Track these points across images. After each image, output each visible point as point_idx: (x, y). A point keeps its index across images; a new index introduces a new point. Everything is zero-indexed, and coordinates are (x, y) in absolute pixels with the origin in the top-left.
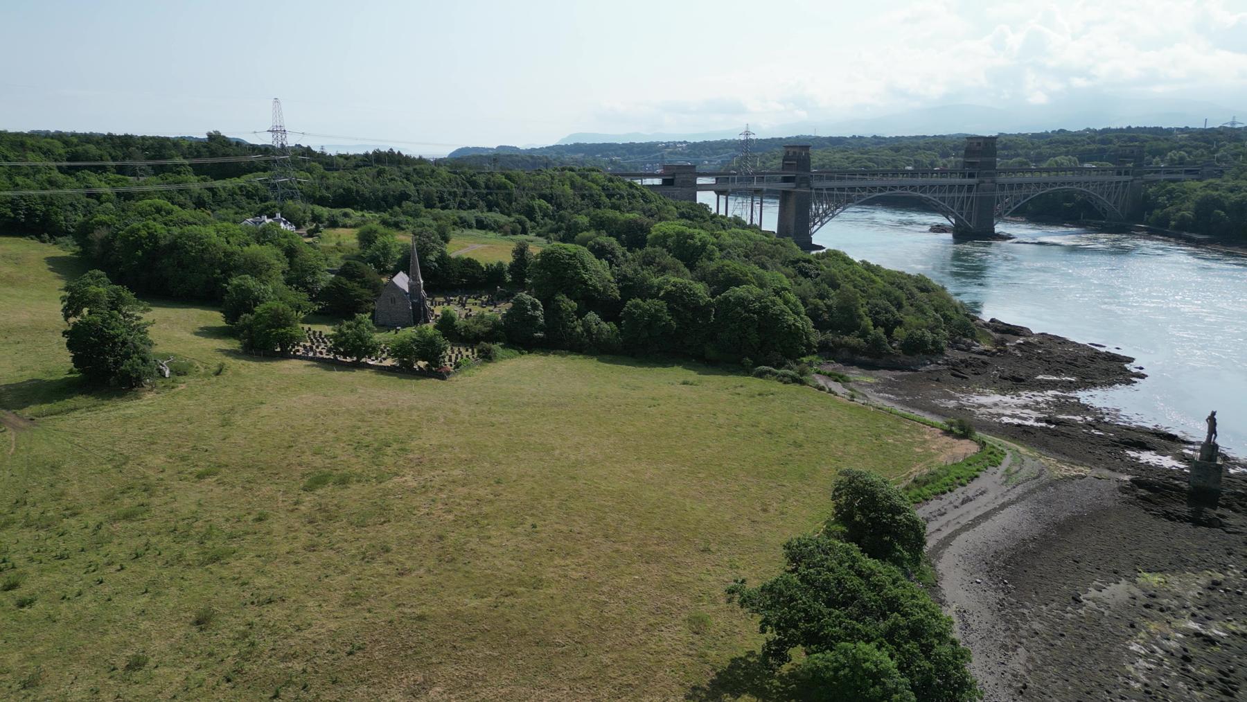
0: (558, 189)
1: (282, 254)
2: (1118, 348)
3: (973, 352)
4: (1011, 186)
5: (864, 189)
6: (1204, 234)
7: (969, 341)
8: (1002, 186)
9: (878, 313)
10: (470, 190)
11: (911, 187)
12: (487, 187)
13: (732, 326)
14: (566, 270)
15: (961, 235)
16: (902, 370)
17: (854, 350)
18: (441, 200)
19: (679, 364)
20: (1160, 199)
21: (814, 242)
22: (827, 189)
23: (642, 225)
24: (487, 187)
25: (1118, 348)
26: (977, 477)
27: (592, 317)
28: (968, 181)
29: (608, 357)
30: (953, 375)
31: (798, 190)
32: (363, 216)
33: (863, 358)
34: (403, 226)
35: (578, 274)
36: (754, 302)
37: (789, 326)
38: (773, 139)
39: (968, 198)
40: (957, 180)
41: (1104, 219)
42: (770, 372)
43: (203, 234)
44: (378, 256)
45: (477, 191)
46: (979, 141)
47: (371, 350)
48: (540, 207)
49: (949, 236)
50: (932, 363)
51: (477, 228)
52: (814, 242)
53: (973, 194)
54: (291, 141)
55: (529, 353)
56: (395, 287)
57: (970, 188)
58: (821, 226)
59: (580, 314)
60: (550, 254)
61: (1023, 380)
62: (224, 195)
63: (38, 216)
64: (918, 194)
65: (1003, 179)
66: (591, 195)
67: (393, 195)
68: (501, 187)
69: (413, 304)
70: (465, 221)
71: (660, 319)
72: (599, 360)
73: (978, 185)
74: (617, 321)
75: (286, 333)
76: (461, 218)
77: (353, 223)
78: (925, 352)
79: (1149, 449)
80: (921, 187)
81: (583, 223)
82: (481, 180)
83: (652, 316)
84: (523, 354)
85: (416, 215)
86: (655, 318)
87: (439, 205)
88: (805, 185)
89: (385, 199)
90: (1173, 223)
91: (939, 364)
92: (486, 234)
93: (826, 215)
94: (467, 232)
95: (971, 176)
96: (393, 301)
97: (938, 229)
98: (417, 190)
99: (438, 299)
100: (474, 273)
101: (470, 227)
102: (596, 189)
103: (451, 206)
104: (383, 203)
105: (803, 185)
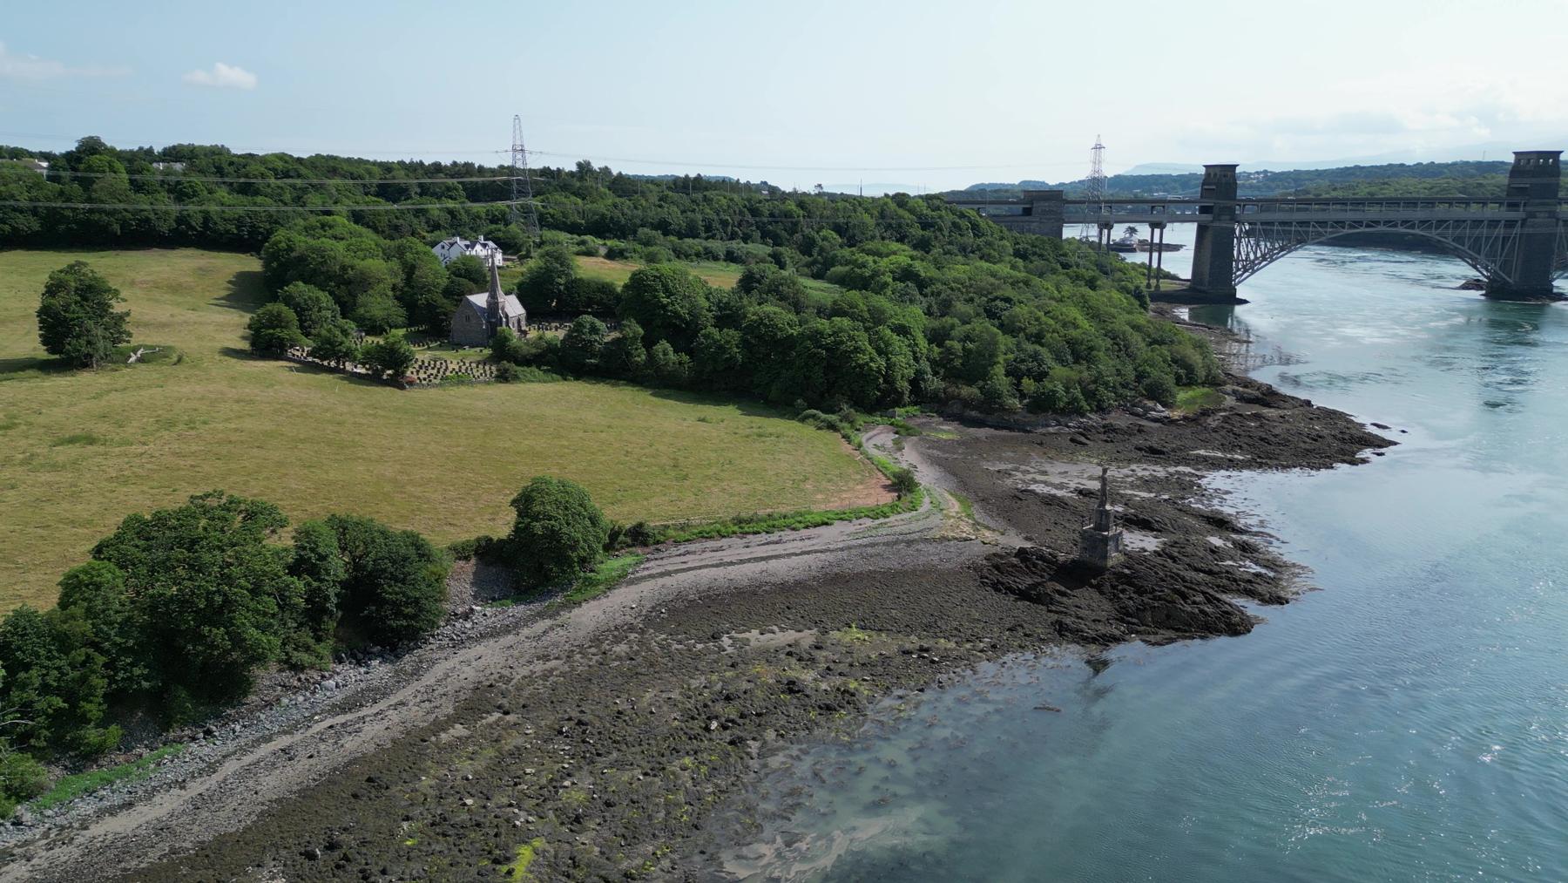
2: (1403, 432)
3: (1147, 419)
5: (1323, 224)
7: (1150, 404)
9: (1023, 361)
10: (749, 217)
12: (772, 215)
15: (1496, 291)
16: (1011, 429)
17: (967, 403)
18: (708, 228)
19: (734, 404)
21: (1238, 296)
22: (1283, 223)
24: (772, 215)
25: (1403, 432)
26: (827, 524)
27: (663, 346)
28: (1512, 215)
29: (666, 392)
30: (1072, 440)
31: (1217, 224)
33: (973, 413)
34: (628, 255)
35: (655, 297)
36: (830, 336)
37: (861, 366)
38: (1390, 165)
39: (1505, 239)
40: (1492, 211)
42: (814, 416)
43: (328, 247)
45: (757, 219)
46: (1529, 157)
47: (348, 355)
49: (1476, 294)
50: (1059, 424)
51: (725, 260)
52: (1238, 296)
53: (1517, 230)
54: (535, 163)
55: (577, 379)
56: (470, 304)
57: (1510, 224)
58: (1252, 274)
59: (649, 342)
61: (1163, 453)
62: (465, 218)
63: (261, 233)
64: (1401, 230)
66: (900, 226)
68: (788, 215)
69: (489, 322)
70: (711, 252)
72: (653, 395)
73: (1524, 221)
74: (690, 353)
75: (272, 334)
76: (706, 249)
78: (1055, 411)
79: (1152, 530)
80: (1423, 222)
82: (765, 209)
83: (721, 347)
84: (566, 380)
85: (647, 243)
86: (721, 349)
87: (703, 235)
88: (1228, 217)
91: (1068, 427)
92: (727, 266)
93: (1264, 259)
94: (712, 264)
95: (1513, 206)
96: (468, 318)
97: (1557, 287)
99: (553, 325)
100: (602, 299)
101: (716, 258)
103: (718, 236)
105: (1223, 217)
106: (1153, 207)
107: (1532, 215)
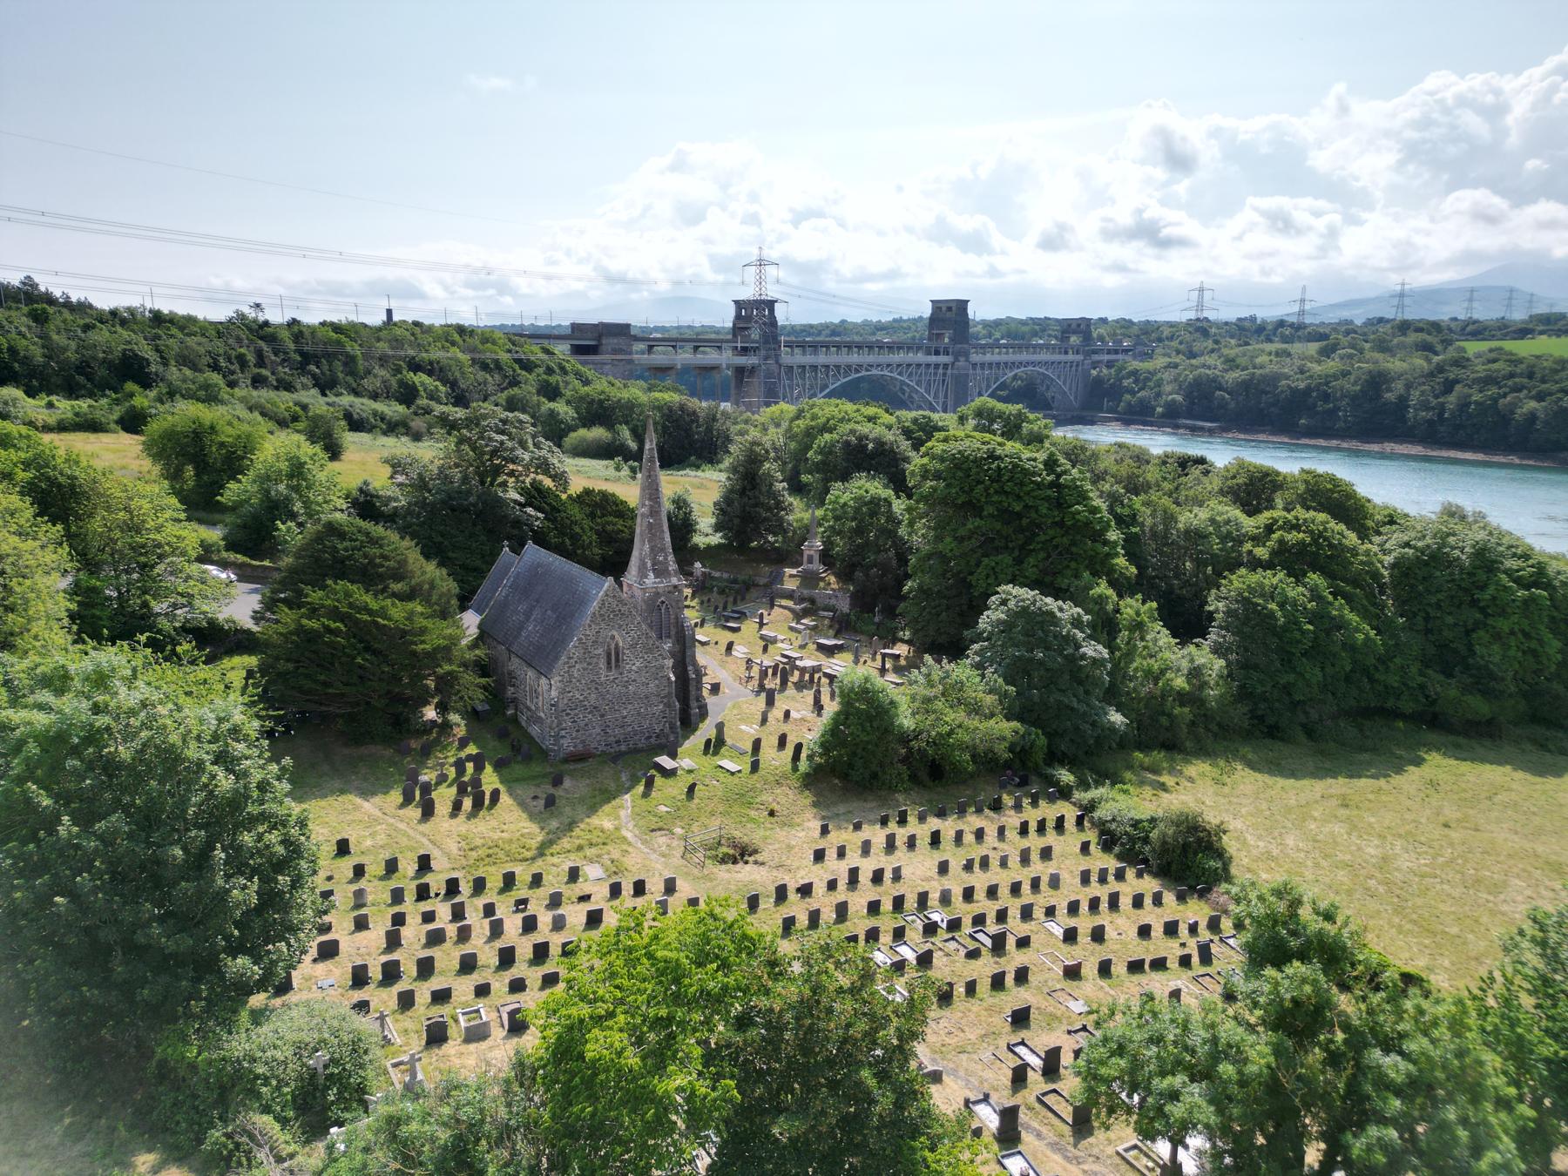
0: (436, 354)
1: (26, 510)
4: (983, 365)
6: (1211, 422)
8: (974, 365)
11: (888, 365)
13: (1504, 625)
14: (1060, 504)
20: (1125, 383)
23: (694, 412)
32: (50, 405)
40: (921, 357)
41: (1051, 409)
44: (288, 499)
48: (423, 384)
57: (946, 366)
60: (982, 458)
65: (976, 358)
67: (104, 360)
71: (1340, 624)
73: (953, 364)
77: (52, 421)
81: (566, 413)
89: (83, 367)
90: (1159, 410)
98: (157, 350)
102: (504, 357)
104: (81, 379)
106: (651, 347)
107: (956, 359)
